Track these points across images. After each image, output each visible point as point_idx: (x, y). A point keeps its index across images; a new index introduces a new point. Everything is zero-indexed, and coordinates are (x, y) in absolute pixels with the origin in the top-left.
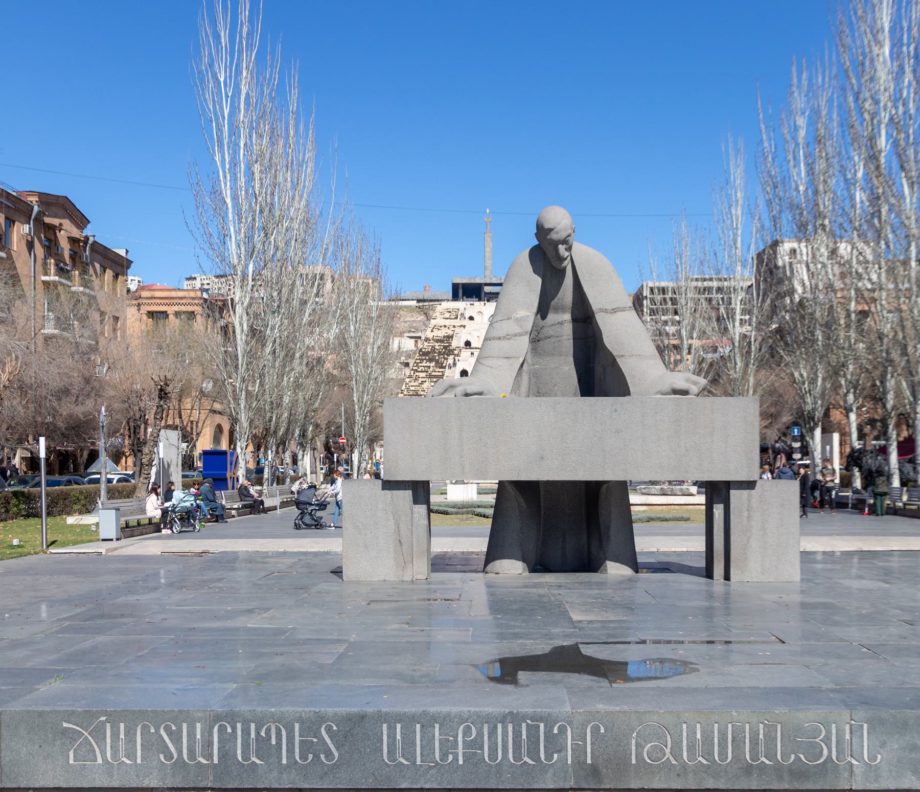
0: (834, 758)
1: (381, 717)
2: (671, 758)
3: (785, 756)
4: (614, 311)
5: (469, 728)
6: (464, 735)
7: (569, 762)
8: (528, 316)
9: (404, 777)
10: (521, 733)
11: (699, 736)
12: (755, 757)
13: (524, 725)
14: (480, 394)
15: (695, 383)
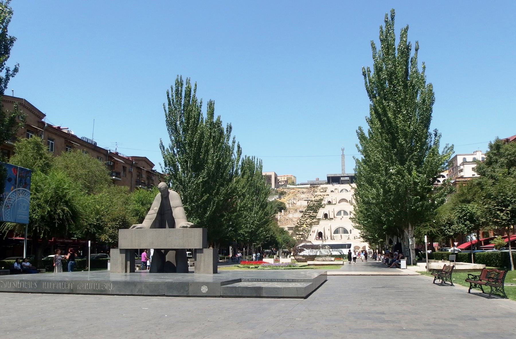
4: (176, 207)
14: (141, 228)
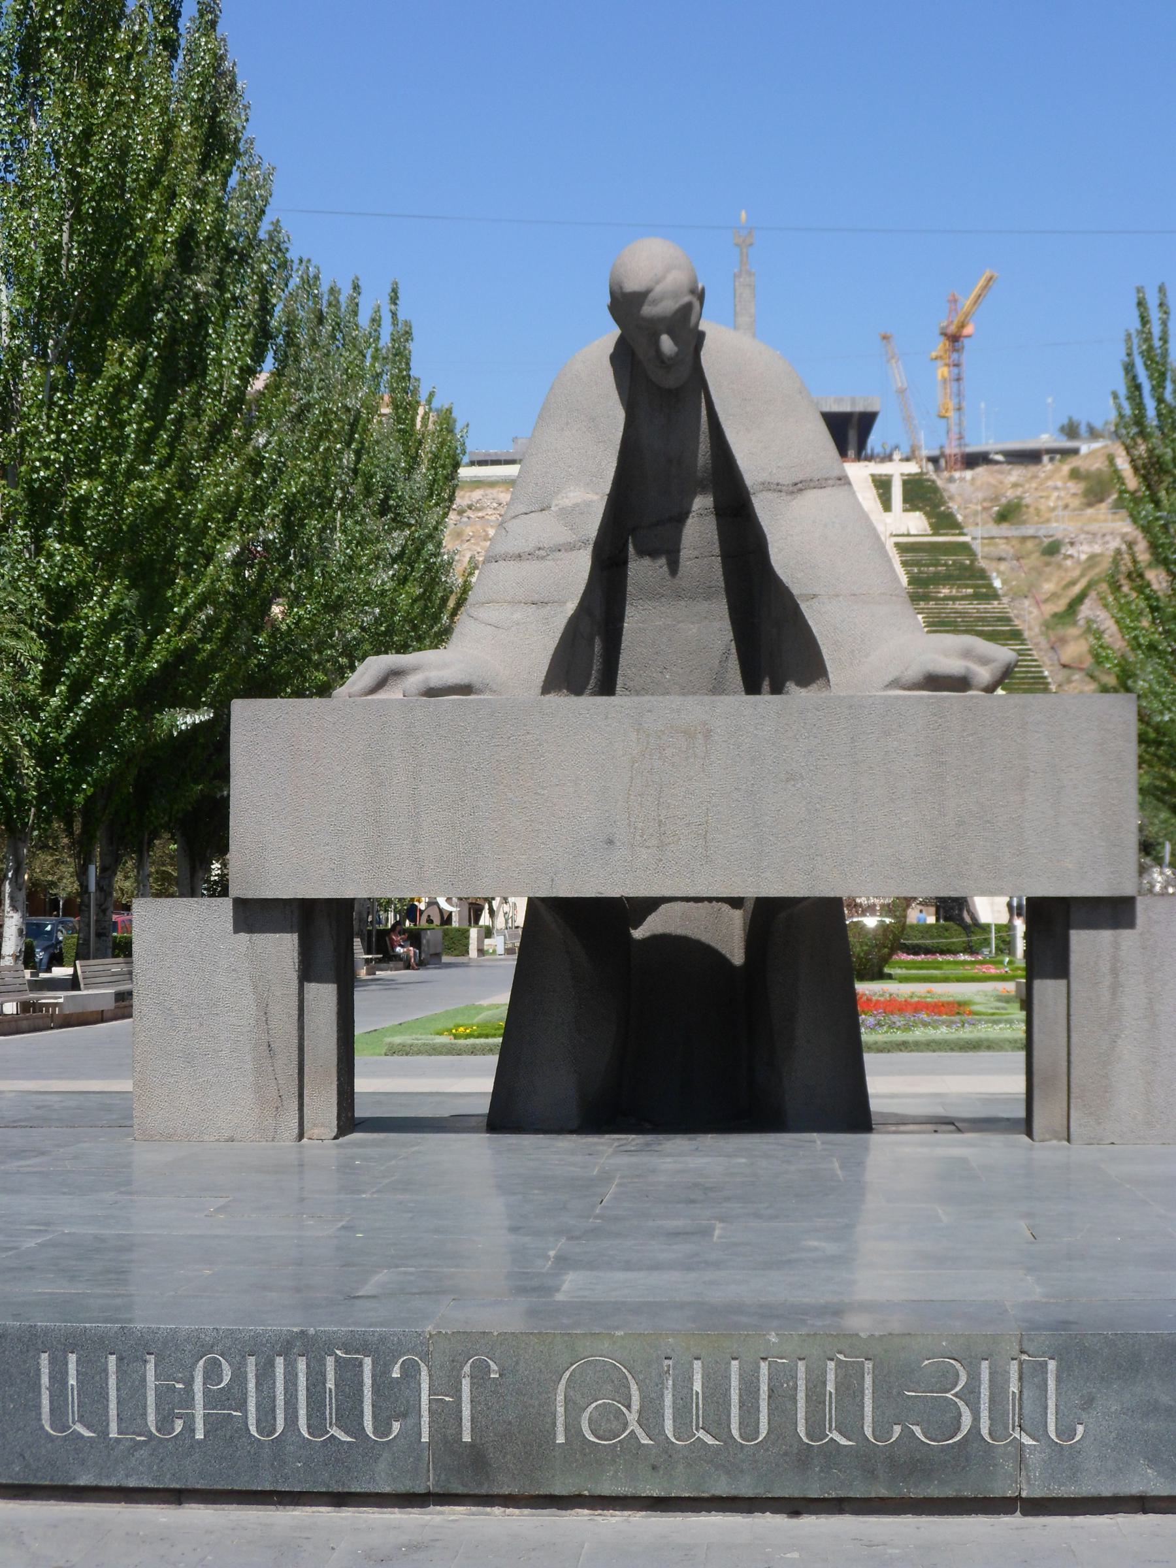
0: (985, 1432)
1: (33, 1341)
2: (640, 1433)
3: (881, 1429)
4: (798, 488)
5: (216, 1364)
6: (207, 1378)
7: (425, 1439)
8: (588, 504)
9: (83, 1462)
10: (324, 1377)
11: (697, 1387)
12: (816, 1430)
13: (330, 1361)
14: (465, 689)
15: (984, 661)
